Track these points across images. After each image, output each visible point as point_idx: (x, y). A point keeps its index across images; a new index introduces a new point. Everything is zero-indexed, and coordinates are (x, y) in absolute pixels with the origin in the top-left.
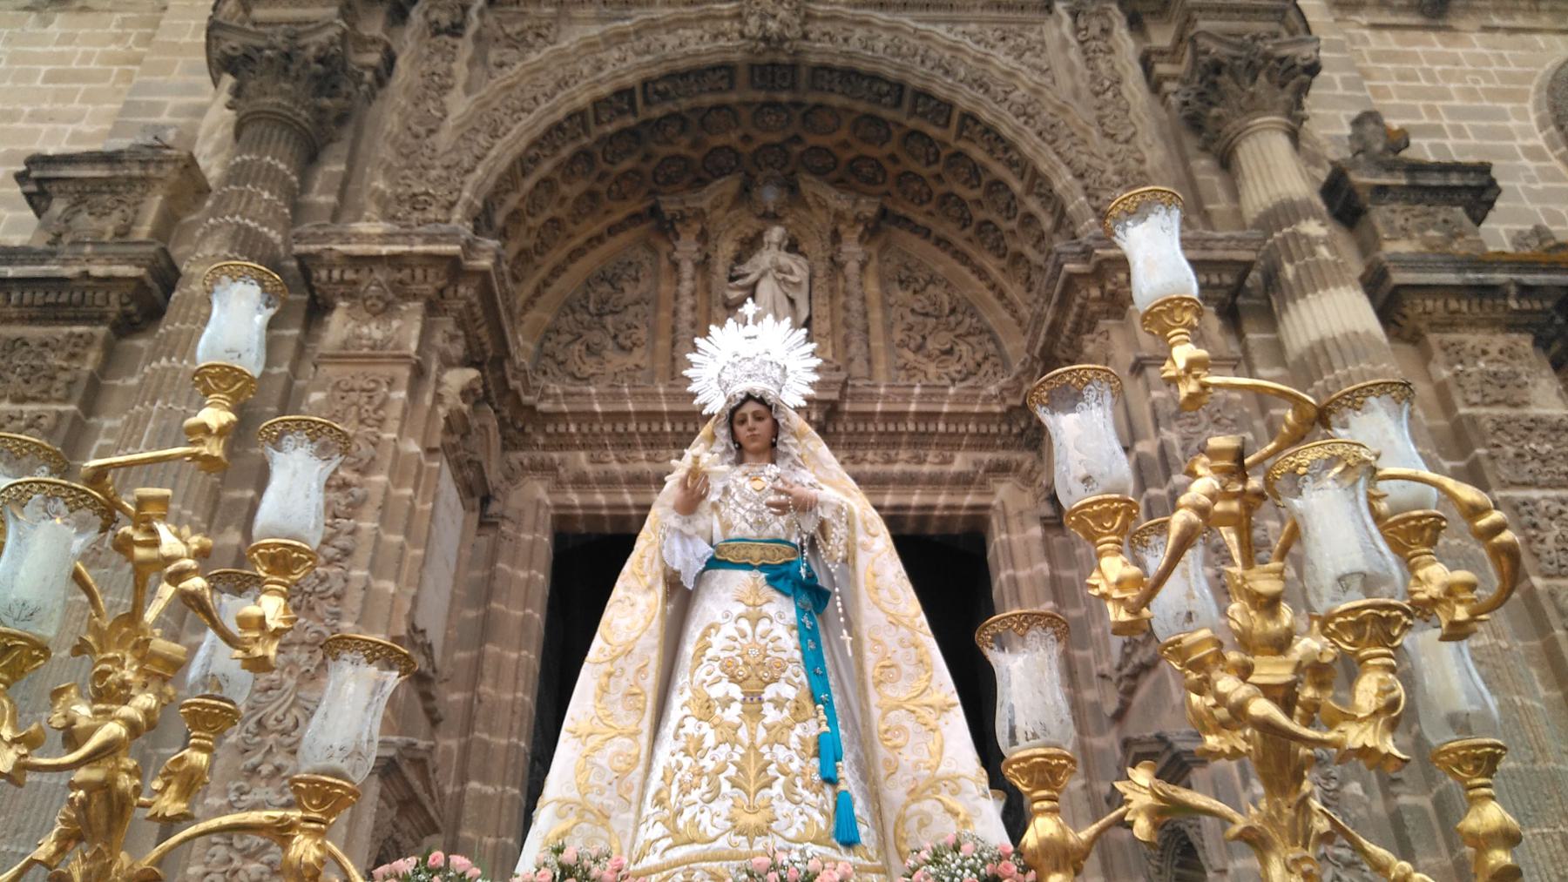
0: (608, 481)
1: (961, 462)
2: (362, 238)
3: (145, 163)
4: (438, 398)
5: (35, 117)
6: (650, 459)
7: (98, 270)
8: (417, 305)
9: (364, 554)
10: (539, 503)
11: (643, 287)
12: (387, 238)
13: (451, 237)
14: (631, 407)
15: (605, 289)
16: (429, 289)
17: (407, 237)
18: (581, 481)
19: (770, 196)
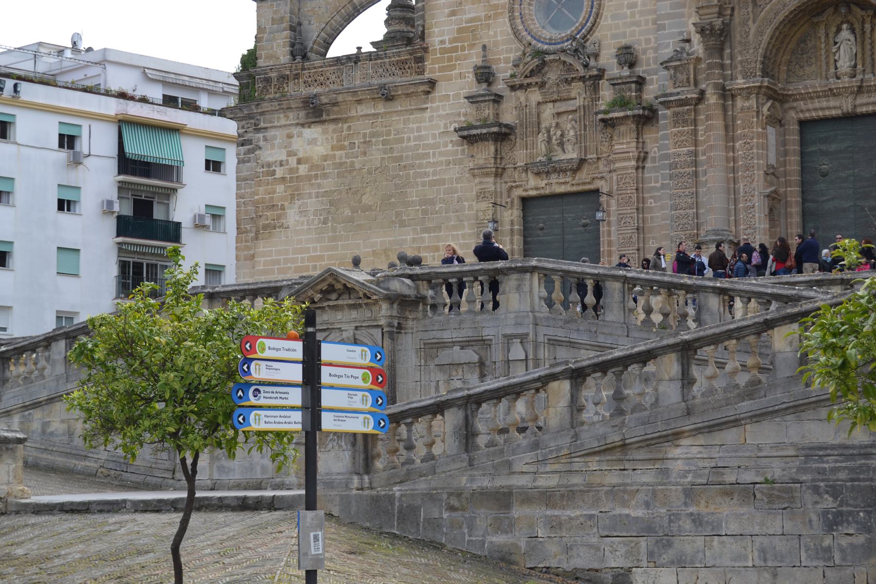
0: (808, 110)
2: (740, 84)
3: (687, 60)
4: (763, 115)
6: (819, 102)
7: (689, 96)
8: (754, 95)
9: (756, 157)
10: (793, 118)
11: (813, 43)
12: (744, 83)
13: (758, 81)
14: (811, 91)
15: (803, 45)
16: (755, 92)
17: (749, 82)
18: (802, 111)
19: (843, 10)
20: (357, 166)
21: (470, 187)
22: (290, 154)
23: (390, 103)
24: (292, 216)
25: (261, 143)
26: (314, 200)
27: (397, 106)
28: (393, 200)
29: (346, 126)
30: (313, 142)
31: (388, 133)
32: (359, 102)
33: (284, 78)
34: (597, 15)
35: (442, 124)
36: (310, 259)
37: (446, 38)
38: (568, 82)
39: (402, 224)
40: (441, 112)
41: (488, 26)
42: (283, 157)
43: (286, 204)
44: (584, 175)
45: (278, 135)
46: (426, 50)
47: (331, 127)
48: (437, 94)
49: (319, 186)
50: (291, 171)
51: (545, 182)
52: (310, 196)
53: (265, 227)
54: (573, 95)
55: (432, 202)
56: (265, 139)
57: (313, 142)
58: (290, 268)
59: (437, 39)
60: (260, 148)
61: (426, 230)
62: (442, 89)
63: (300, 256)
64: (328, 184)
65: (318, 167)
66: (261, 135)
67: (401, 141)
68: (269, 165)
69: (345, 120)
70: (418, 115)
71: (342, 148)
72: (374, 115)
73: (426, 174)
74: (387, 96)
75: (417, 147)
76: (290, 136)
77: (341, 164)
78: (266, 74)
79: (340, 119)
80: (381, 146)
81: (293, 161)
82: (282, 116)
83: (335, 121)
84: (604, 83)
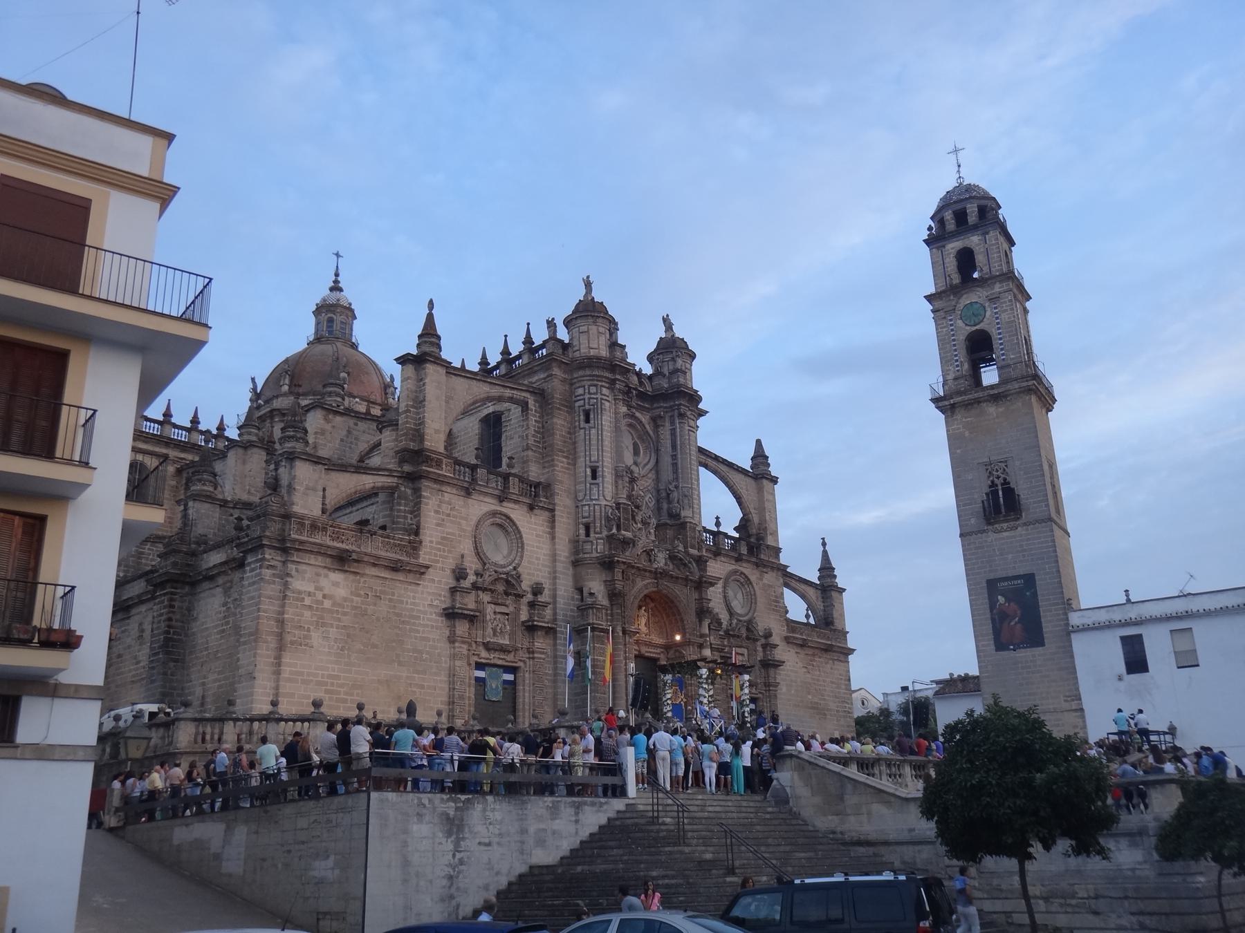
1: (658, 651)
5: (537, 547)
20: (369, 612)
21: (443, 648)
22: (318, 588)
23: (395, 573)
24: (316, 638)
25: (293, 573)
26: (335, 630)
27: (400, 576)
28: (394, 644)
29: (362, 580)
30: (336, 584)
31: (393, 594)
32: (374, 565)
33: (314, 527)
34: (522, 557)
35: (429, 598)
36: (330, 676)
37: (434, 539)
38: (507, 594)
39: (400, 664)
40: (429, 590)
41: (460, 542)
42: (312, 589)
43: (312, 628)
44: (510, 657)
45: (309, 572)
46: (421, 542)
47: (352, 577)
48: (426, 576)
49: (339, 620)
50: (318, 602)
51: (492, 656)
52: (332, 626)
53: (292, 643)
54: (508, 602)
55: (420, 652)
56: (297, 570)
57: (336, 584)
58: (312, 680)
59: (429, 539)
60: (292, 577)
61: (417, 672)
62: (431, 574)
63: (320, 672)
64: (346, 620)
65: (340, 605)
66: (294, 567)
67: (402, 602)
68: (300, 592)
69: (363, 575)
70: (413, 587)
71: (359, 595)
72: (383, 578)
73: (418, 632)
74: (395, 567)
75: (412, 610)
76: (318, 575)
77: (356, 608)
78: (303, 519)
79: (358, 573)
80: (387, 602)
81: (319, 596)
82: (312, 556)
83: (356, 573)
84: (525, 600)
